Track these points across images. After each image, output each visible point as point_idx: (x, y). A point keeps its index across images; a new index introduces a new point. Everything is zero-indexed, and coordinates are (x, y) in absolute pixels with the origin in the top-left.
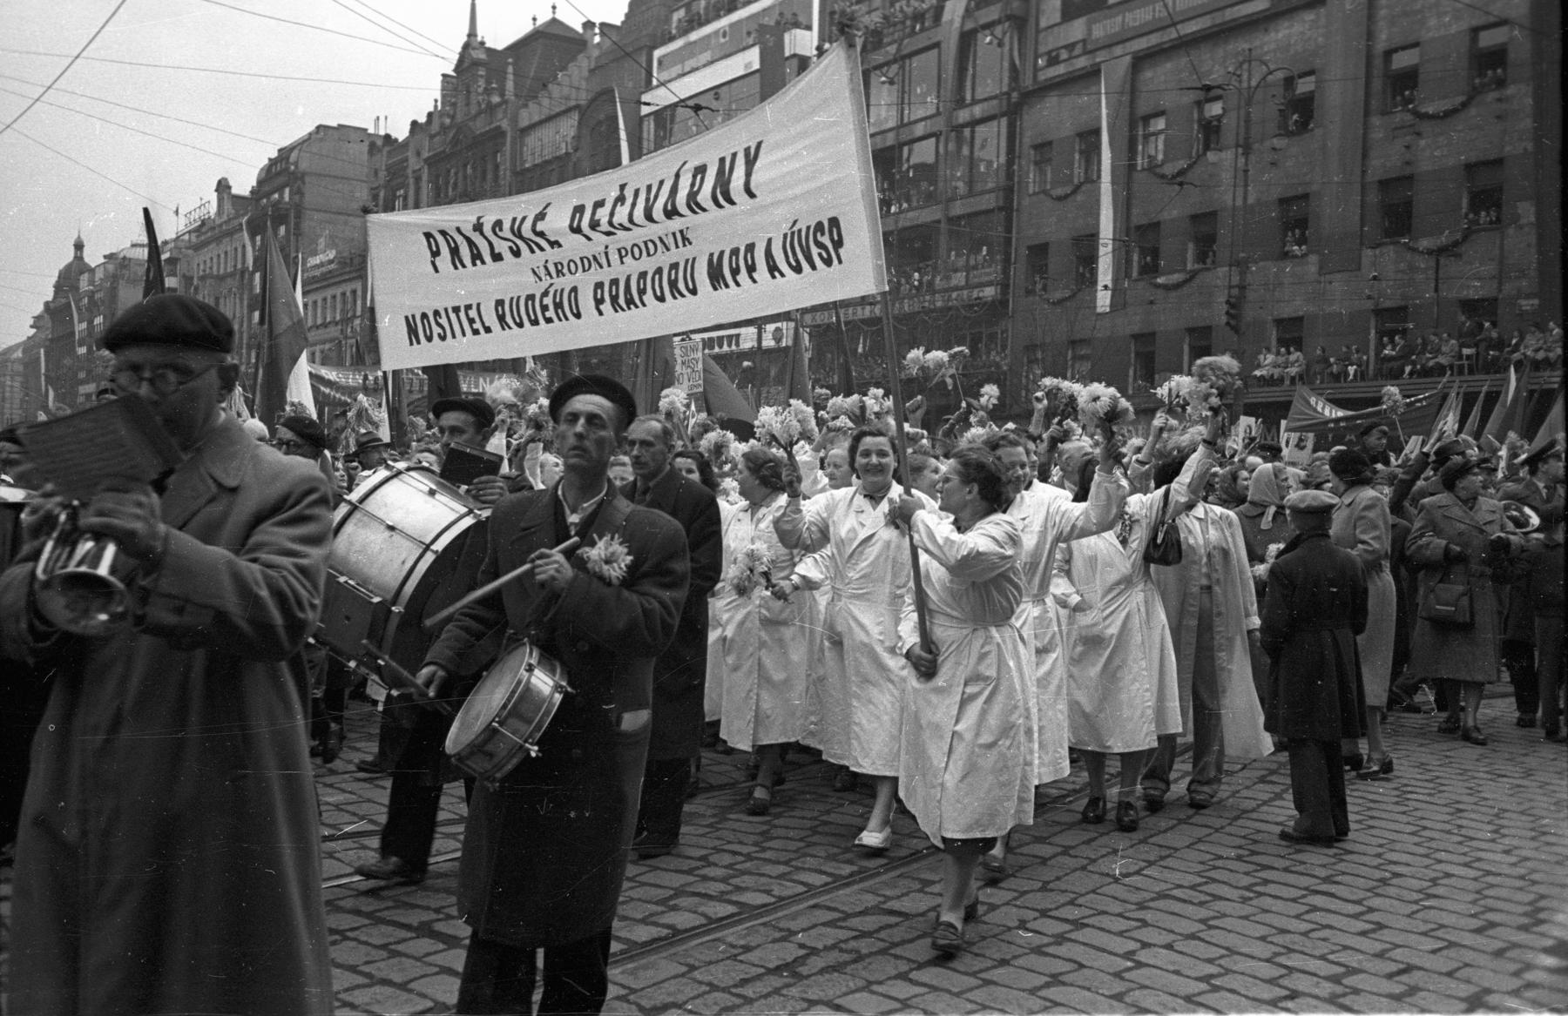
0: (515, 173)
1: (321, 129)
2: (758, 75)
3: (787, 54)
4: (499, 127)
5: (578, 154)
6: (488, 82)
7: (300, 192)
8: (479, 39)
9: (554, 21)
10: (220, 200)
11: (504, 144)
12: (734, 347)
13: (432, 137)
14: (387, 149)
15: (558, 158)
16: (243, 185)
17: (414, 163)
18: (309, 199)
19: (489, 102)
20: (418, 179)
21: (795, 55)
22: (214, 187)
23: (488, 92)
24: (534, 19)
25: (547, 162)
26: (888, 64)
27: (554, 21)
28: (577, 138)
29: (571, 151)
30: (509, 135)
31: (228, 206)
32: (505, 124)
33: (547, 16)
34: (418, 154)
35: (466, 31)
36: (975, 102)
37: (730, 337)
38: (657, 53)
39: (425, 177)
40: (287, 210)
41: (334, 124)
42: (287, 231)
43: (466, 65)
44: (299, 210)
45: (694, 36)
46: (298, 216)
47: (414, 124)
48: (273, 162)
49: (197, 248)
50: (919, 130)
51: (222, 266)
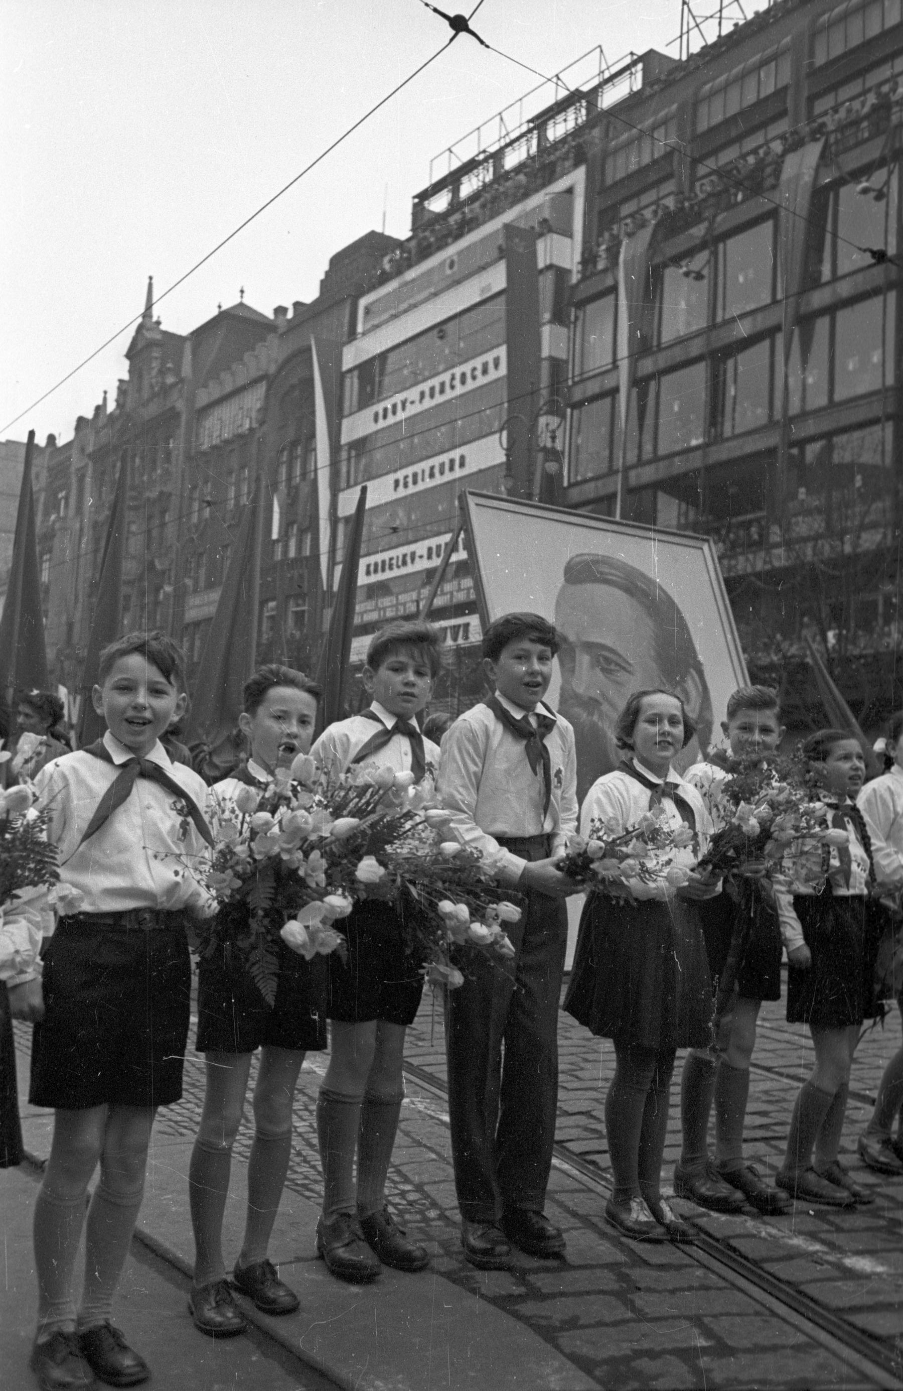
0: (189, 458)
2: (503, 298)
3: (541, 265)
4: (173, 408)
5: (265, 428)
6: (163, 363)
8: (155, 319)
9: (241, 305)
11: (178, 426)
12: (460, 641)
15: (240, 436)
17: (76, 461)
19: (164, 383)
20: (81, 480)
21: (550, 267)
23: (162, 372)
24: (220, 307)
25: (227, 442)
26: (690, 253)
27: (241, 305)
28: (264, 410)
29: (255, 425)
30: (184, 418)
32: (180, 405)
33: (236, 301)
35: (142, 310)
36: (835, 278)
37: (455, 629)
38: (363, 302)
39: (90, 472)
43: (139, 346)
45: (411, 274)
47: (81, 420)
50: (743, 329)
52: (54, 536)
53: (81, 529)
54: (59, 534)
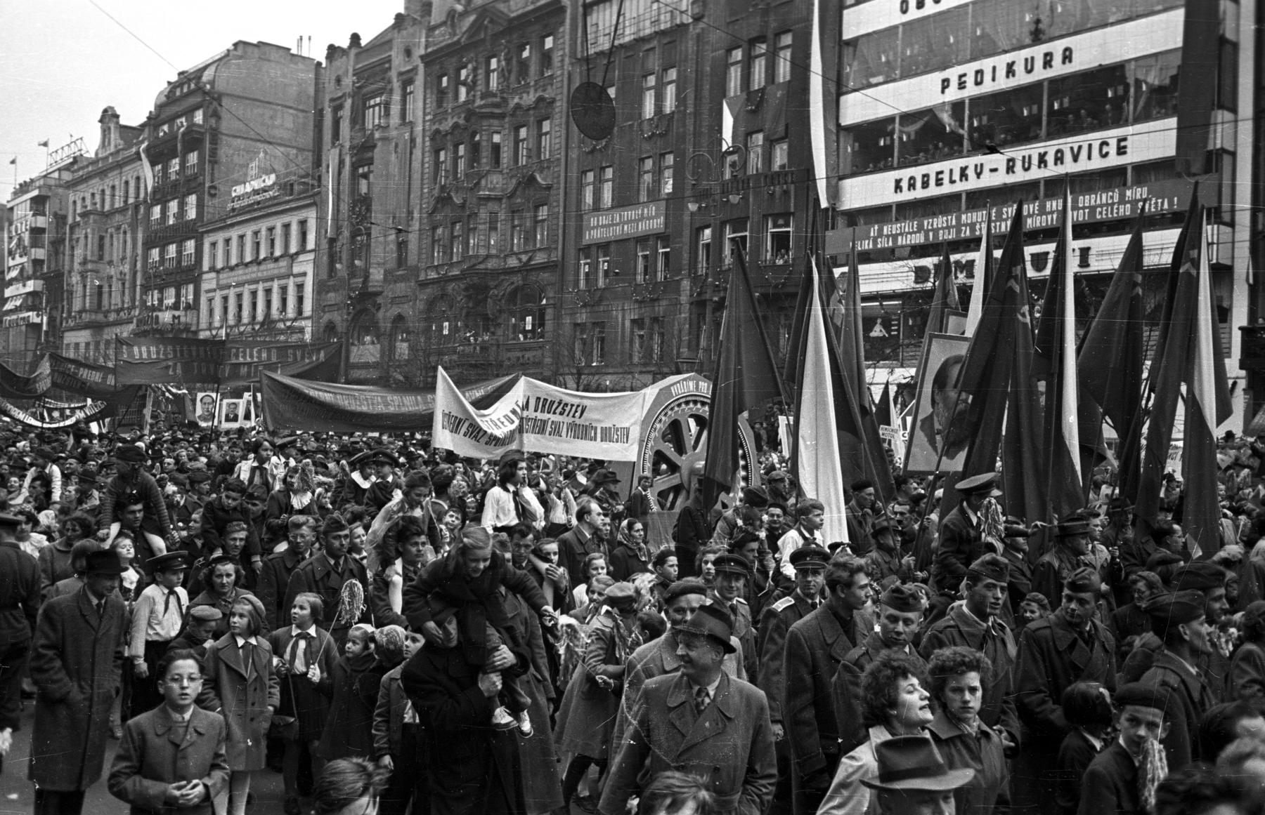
1: (240, 47)
7: (216, 115)
10: (105, 132)
11: (562, 23)
13: (431, 29)
14: (354, 51)
16: (135, 114)
17: (399, 63)
18: (226, 125)
22: (99, 116)
31: (114, 136)
34: (408, 52)
40: (202, 134)
41: (255, 42)
42: (201, 158)
44: (215, 135)
46: (214, 141)
48: (173, 86)
49: (71, 185)
51: (108, 198)
52: (374, 146)
53: (413, 140)
54: (379, 144)
